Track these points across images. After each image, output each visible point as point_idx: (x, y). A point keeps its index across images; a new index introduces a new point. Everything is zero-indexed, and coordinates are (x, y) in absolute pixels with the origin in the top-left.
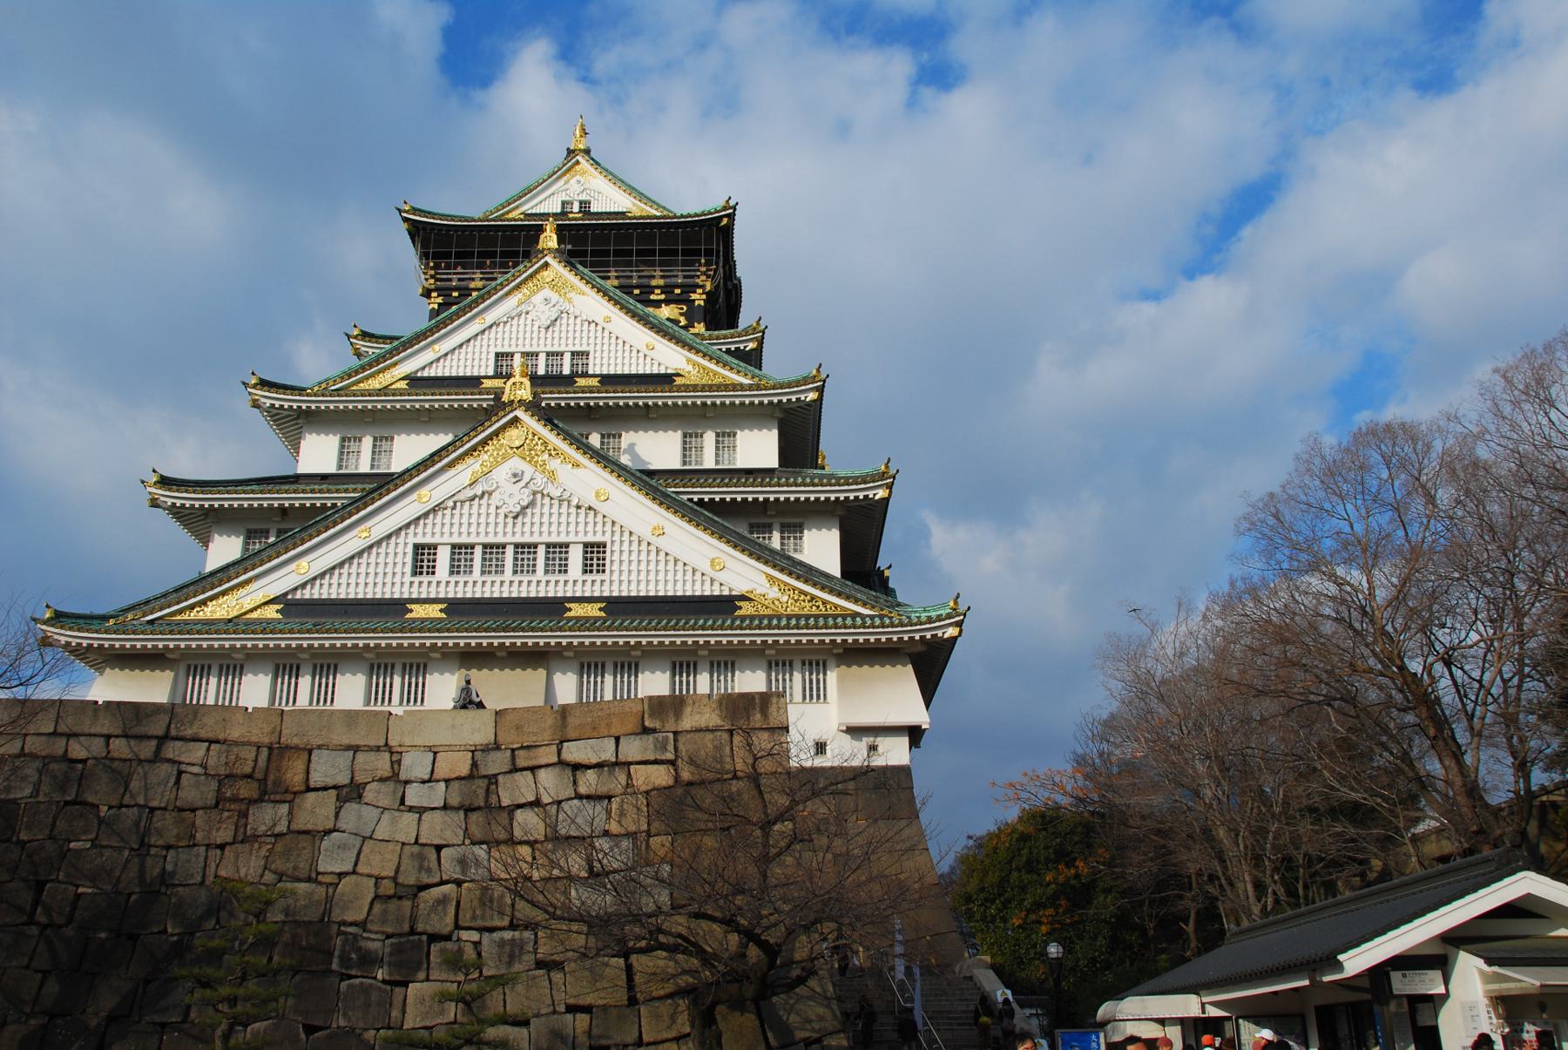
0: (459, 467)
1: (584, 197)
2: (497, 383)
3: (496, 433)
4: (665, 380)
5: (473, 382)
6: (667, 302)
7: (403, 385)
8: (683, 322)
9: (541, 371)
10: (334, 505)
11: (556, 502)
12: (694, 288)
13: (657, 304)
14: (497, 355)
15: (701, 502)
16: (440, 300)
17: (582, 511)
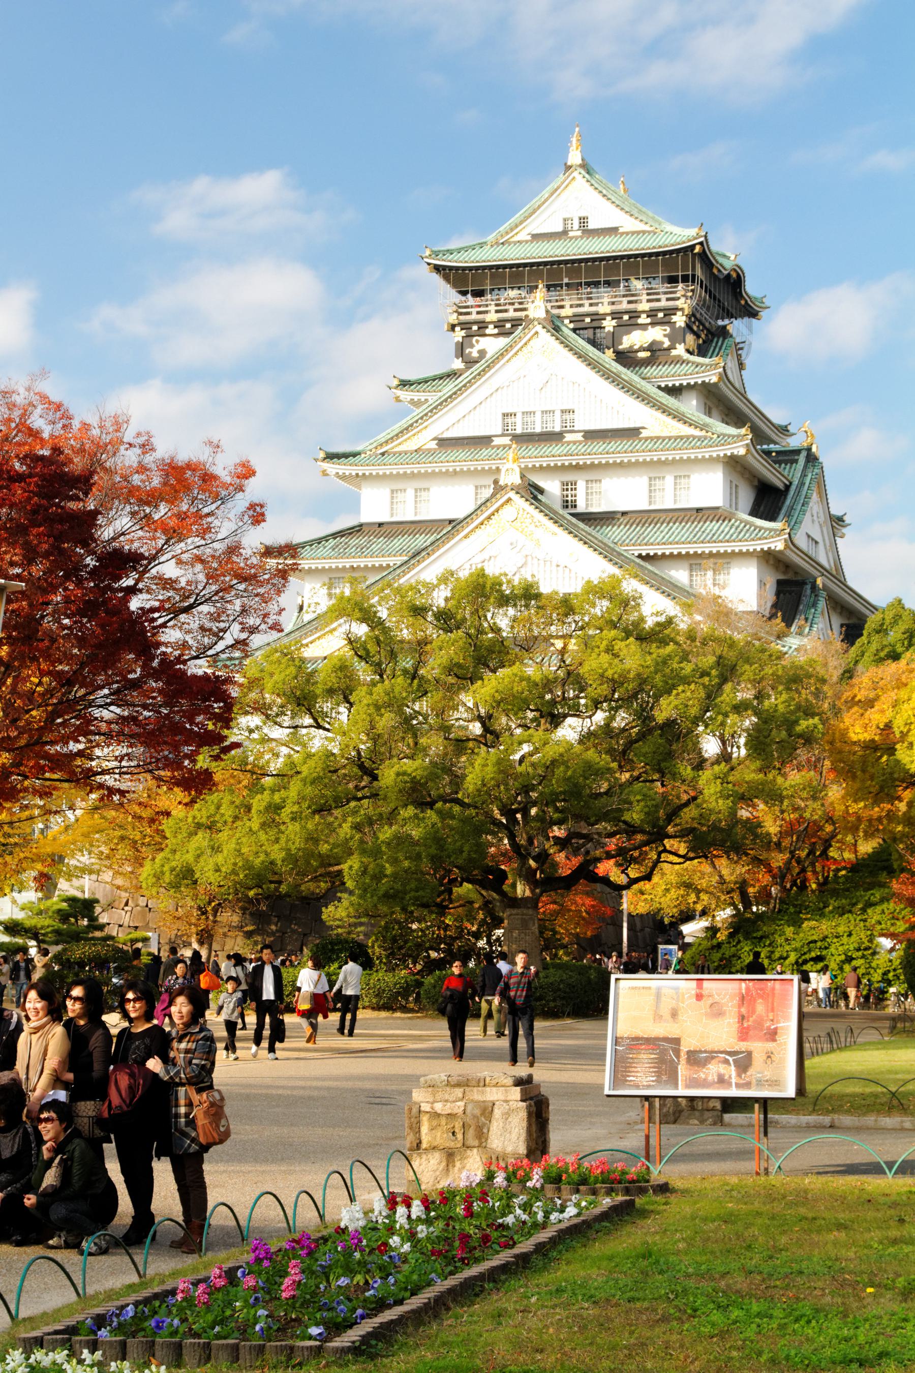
0: (473, 537)
1: (582, 215)
2: (506, 440)
3: (497, 511)
4: (632, 433)
5: (484, 441)
6: (653, 324)
7: (433, 445)
8: (667, 343)
9: (538, 430)
10: (388, 565)
11: (542, 562)
12: (672, 311)
13: (644, 327)
14: (504, 415)
15: (647, 558)
16: (463, 333)
17: (560, 569)
